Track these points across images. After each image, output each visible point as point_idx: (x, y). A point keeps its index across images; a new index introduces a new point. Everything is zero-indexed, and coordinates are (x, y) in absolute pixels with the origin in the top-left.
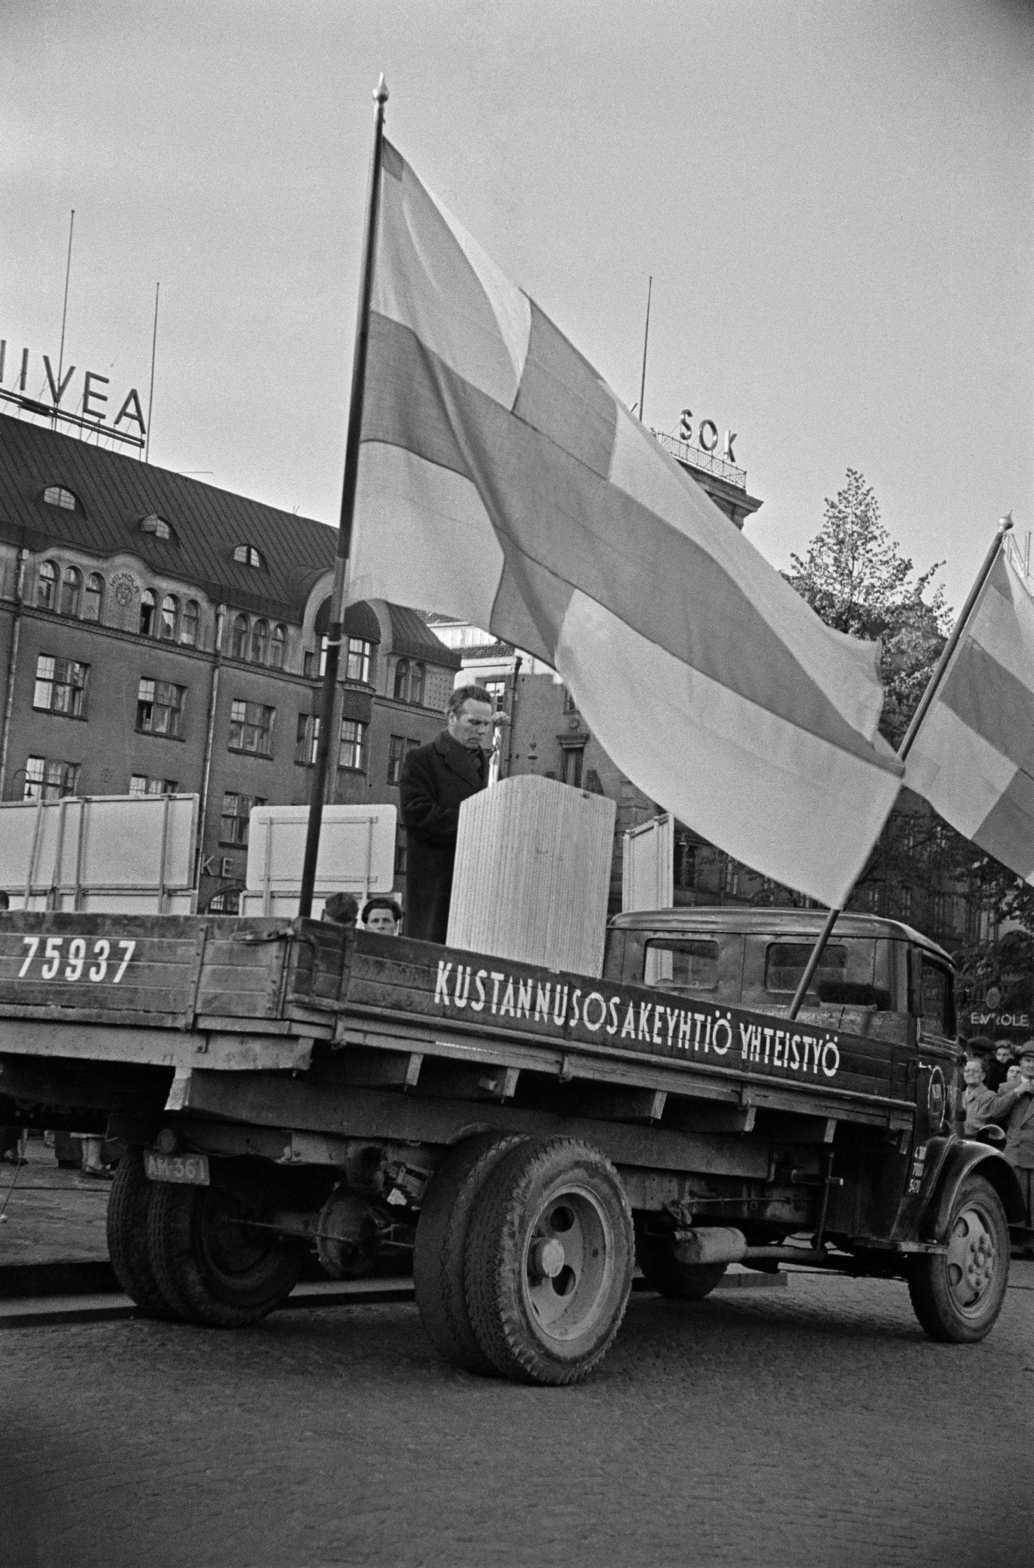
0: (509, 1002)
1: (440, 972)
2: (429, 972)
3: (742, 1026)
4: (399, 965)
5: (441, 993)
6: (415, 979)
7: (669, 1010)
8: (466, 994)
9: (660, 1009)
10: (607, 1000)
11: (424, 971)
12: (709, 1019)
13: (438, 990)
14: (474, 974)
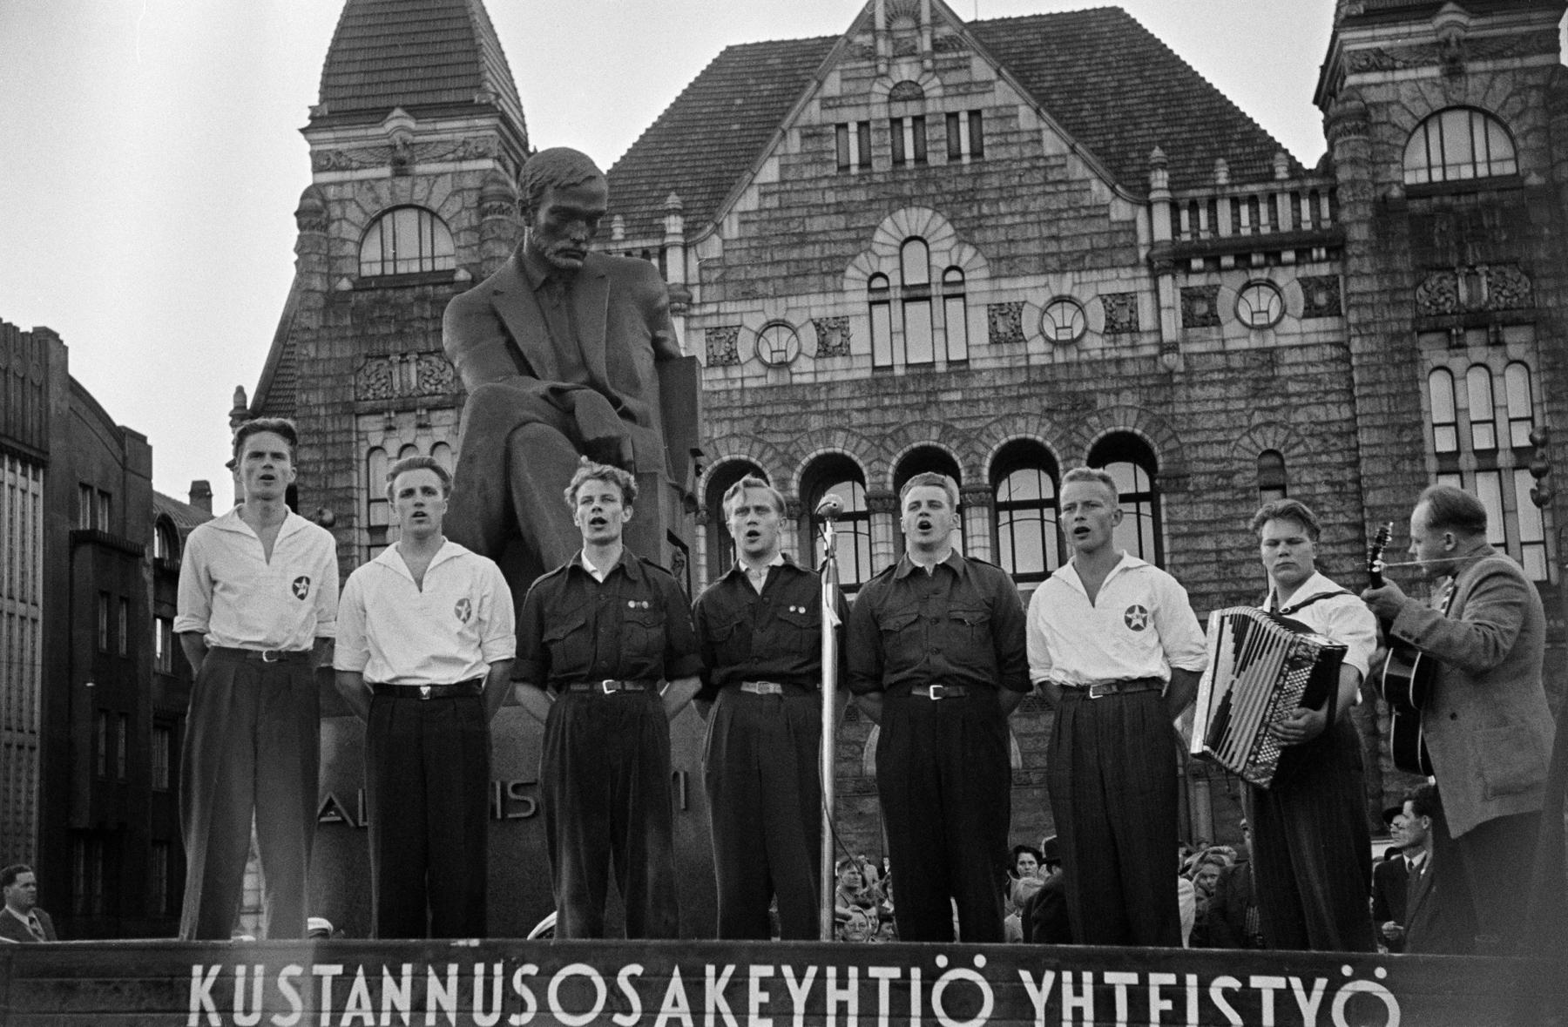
0: (359, 1005)
1: (196, 982)
2: (170, 984)
3: (1025, 975)
4: (108, 983)
5: (203, 1011)
6: (142, 999)
7: (787, 970)
8: (257, 1004)
9: (758, 972)
10: (610, 975)
11: (158, 985)
12: (916, 973)
13: (194, 1005)
14: (272, 974)
